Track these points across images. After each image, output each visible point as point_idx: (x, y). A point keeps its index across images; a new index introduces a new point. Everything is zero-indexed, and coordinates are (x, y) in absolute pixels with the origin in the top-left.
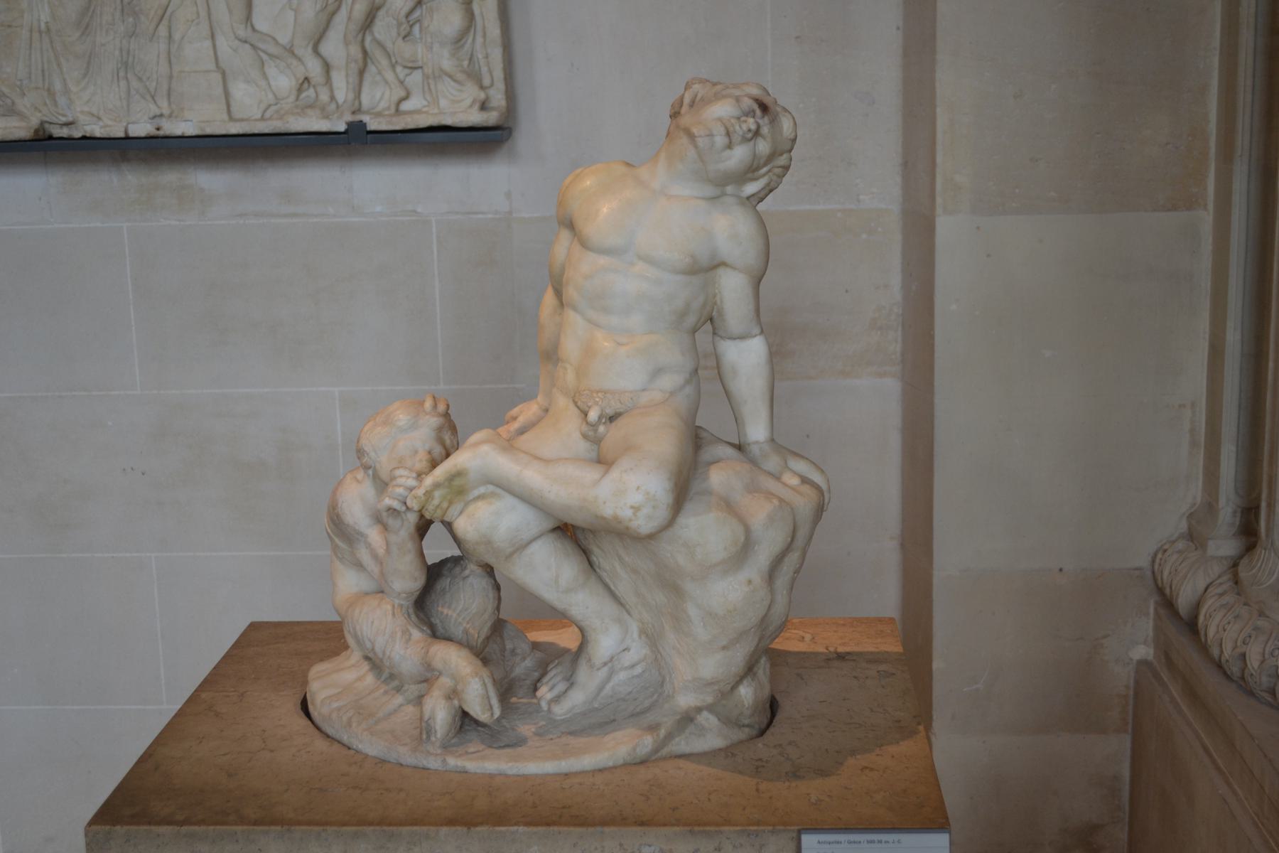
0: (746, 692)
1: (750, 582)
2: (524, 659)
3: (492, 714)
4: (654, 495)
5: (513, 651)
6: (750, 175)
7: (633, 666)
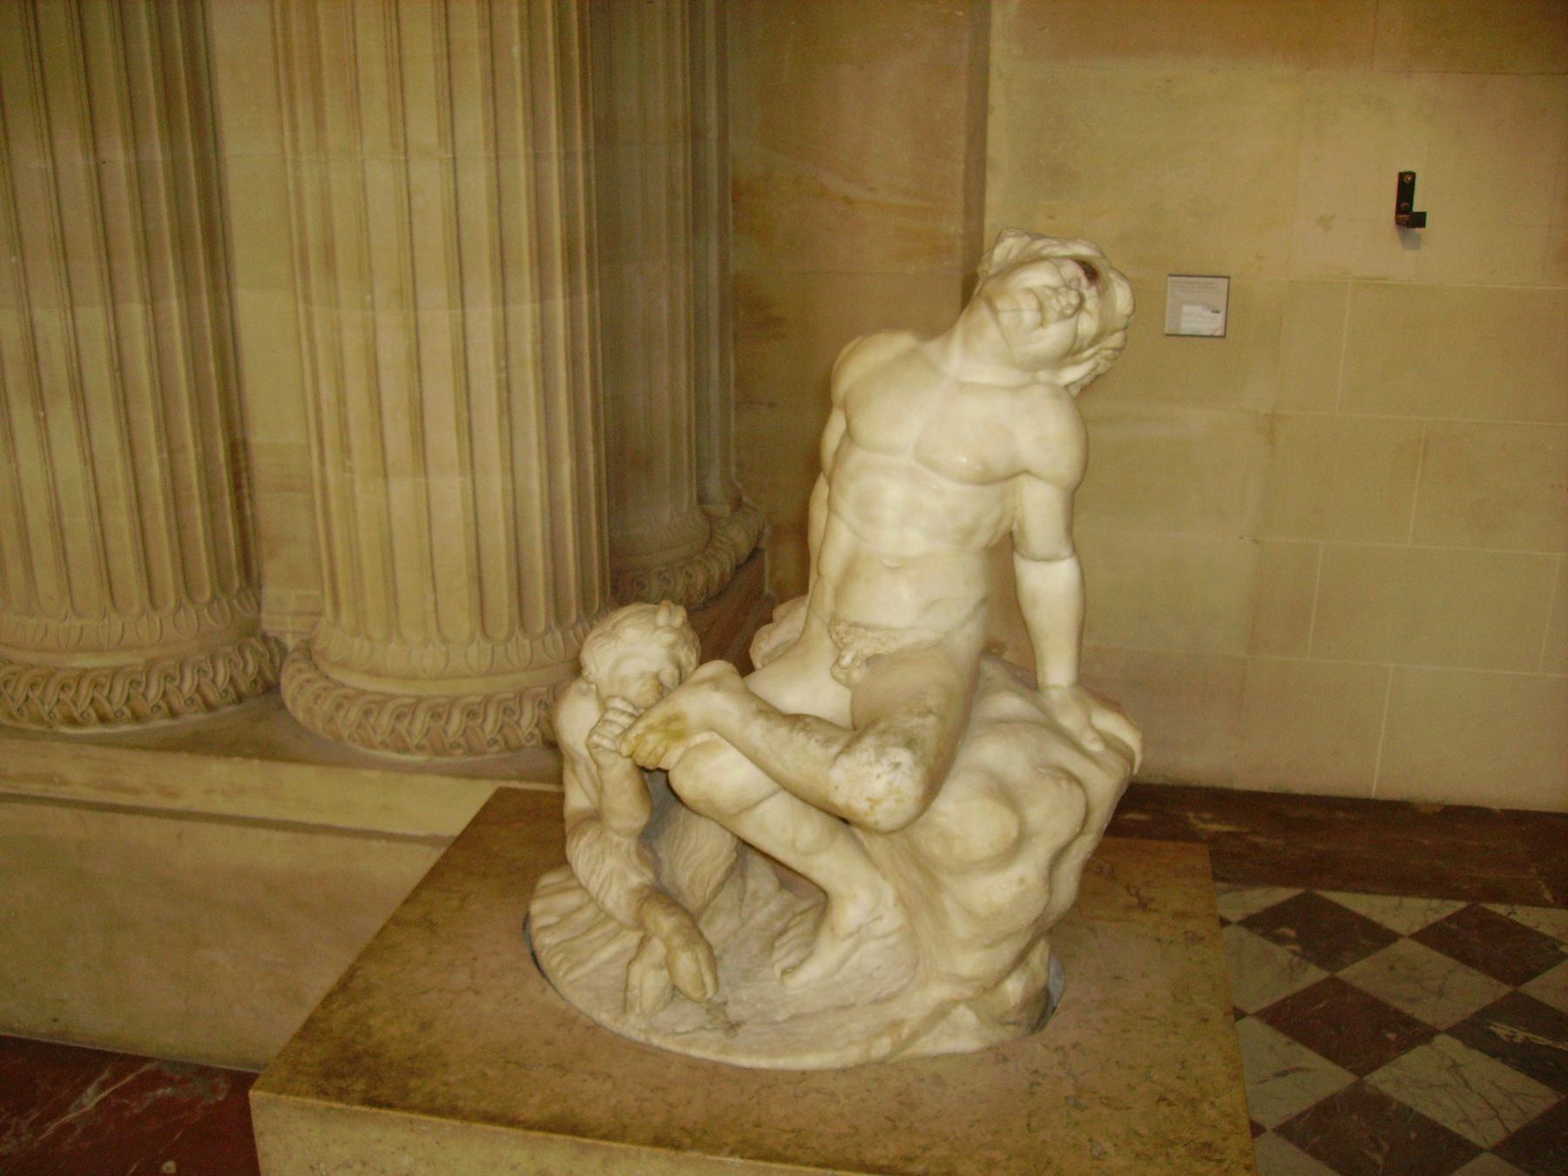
0: (1014, 989)
1: (1022, 881)
2: (767, 903)
3: (705, 994)
4: (898, 788)
5: (755, 893)
6: (1069, 359)
7: (884, 936)
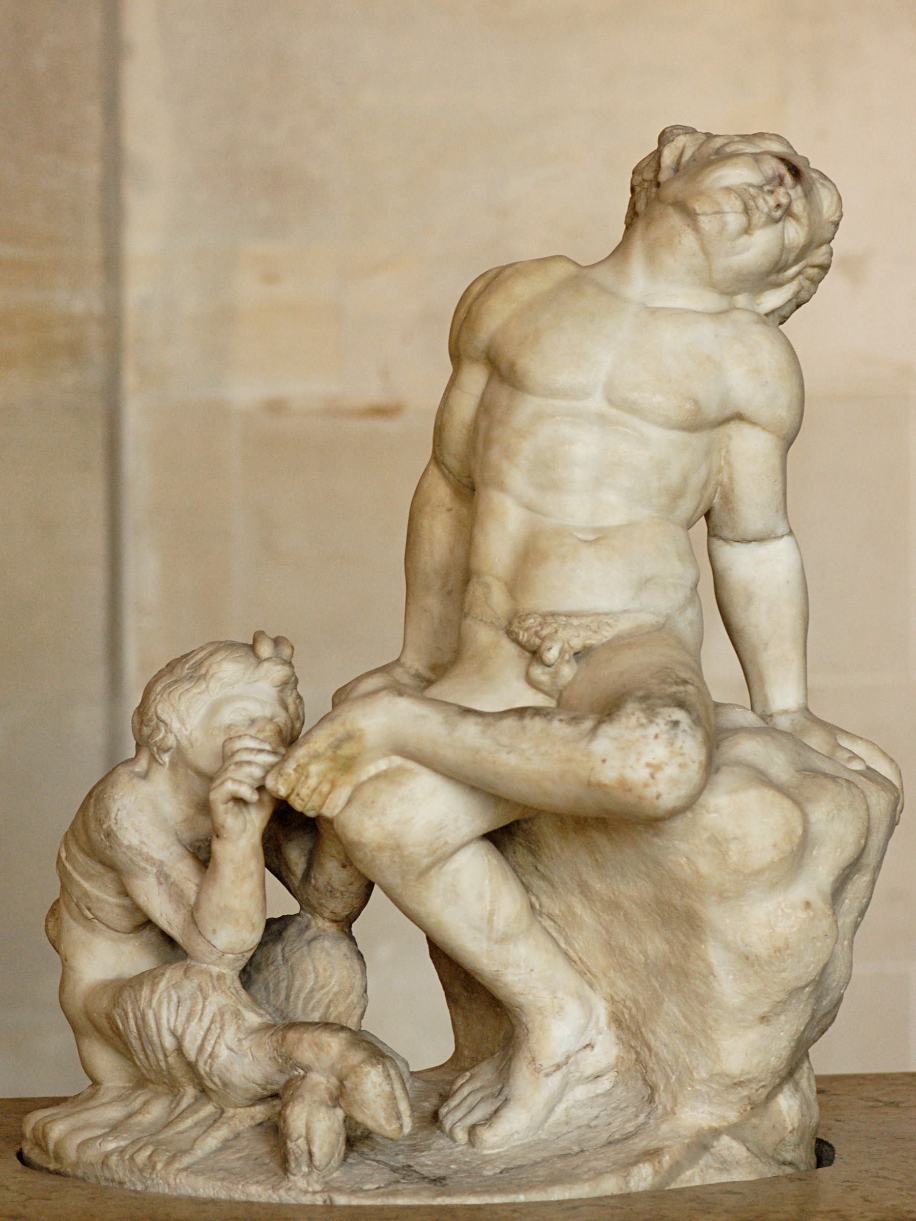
1: (808, 905)
6: (773, 278)
